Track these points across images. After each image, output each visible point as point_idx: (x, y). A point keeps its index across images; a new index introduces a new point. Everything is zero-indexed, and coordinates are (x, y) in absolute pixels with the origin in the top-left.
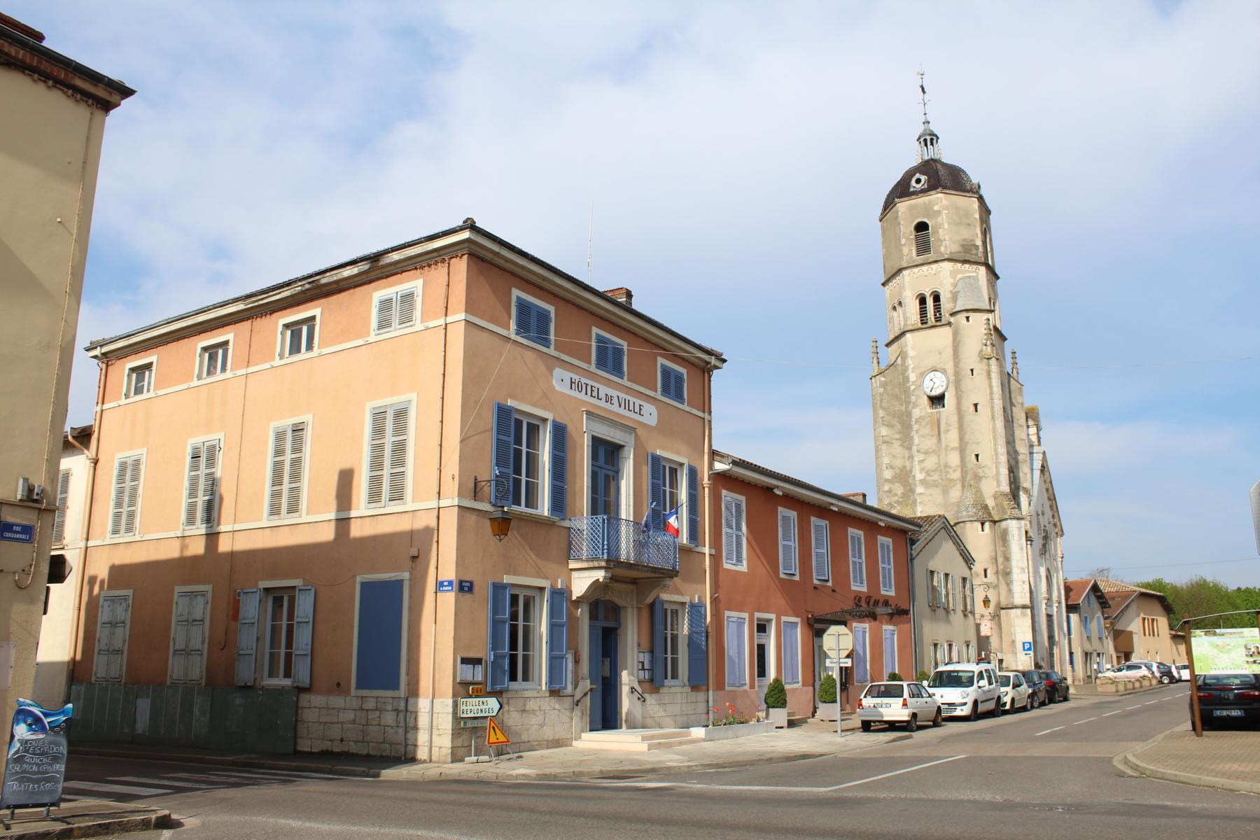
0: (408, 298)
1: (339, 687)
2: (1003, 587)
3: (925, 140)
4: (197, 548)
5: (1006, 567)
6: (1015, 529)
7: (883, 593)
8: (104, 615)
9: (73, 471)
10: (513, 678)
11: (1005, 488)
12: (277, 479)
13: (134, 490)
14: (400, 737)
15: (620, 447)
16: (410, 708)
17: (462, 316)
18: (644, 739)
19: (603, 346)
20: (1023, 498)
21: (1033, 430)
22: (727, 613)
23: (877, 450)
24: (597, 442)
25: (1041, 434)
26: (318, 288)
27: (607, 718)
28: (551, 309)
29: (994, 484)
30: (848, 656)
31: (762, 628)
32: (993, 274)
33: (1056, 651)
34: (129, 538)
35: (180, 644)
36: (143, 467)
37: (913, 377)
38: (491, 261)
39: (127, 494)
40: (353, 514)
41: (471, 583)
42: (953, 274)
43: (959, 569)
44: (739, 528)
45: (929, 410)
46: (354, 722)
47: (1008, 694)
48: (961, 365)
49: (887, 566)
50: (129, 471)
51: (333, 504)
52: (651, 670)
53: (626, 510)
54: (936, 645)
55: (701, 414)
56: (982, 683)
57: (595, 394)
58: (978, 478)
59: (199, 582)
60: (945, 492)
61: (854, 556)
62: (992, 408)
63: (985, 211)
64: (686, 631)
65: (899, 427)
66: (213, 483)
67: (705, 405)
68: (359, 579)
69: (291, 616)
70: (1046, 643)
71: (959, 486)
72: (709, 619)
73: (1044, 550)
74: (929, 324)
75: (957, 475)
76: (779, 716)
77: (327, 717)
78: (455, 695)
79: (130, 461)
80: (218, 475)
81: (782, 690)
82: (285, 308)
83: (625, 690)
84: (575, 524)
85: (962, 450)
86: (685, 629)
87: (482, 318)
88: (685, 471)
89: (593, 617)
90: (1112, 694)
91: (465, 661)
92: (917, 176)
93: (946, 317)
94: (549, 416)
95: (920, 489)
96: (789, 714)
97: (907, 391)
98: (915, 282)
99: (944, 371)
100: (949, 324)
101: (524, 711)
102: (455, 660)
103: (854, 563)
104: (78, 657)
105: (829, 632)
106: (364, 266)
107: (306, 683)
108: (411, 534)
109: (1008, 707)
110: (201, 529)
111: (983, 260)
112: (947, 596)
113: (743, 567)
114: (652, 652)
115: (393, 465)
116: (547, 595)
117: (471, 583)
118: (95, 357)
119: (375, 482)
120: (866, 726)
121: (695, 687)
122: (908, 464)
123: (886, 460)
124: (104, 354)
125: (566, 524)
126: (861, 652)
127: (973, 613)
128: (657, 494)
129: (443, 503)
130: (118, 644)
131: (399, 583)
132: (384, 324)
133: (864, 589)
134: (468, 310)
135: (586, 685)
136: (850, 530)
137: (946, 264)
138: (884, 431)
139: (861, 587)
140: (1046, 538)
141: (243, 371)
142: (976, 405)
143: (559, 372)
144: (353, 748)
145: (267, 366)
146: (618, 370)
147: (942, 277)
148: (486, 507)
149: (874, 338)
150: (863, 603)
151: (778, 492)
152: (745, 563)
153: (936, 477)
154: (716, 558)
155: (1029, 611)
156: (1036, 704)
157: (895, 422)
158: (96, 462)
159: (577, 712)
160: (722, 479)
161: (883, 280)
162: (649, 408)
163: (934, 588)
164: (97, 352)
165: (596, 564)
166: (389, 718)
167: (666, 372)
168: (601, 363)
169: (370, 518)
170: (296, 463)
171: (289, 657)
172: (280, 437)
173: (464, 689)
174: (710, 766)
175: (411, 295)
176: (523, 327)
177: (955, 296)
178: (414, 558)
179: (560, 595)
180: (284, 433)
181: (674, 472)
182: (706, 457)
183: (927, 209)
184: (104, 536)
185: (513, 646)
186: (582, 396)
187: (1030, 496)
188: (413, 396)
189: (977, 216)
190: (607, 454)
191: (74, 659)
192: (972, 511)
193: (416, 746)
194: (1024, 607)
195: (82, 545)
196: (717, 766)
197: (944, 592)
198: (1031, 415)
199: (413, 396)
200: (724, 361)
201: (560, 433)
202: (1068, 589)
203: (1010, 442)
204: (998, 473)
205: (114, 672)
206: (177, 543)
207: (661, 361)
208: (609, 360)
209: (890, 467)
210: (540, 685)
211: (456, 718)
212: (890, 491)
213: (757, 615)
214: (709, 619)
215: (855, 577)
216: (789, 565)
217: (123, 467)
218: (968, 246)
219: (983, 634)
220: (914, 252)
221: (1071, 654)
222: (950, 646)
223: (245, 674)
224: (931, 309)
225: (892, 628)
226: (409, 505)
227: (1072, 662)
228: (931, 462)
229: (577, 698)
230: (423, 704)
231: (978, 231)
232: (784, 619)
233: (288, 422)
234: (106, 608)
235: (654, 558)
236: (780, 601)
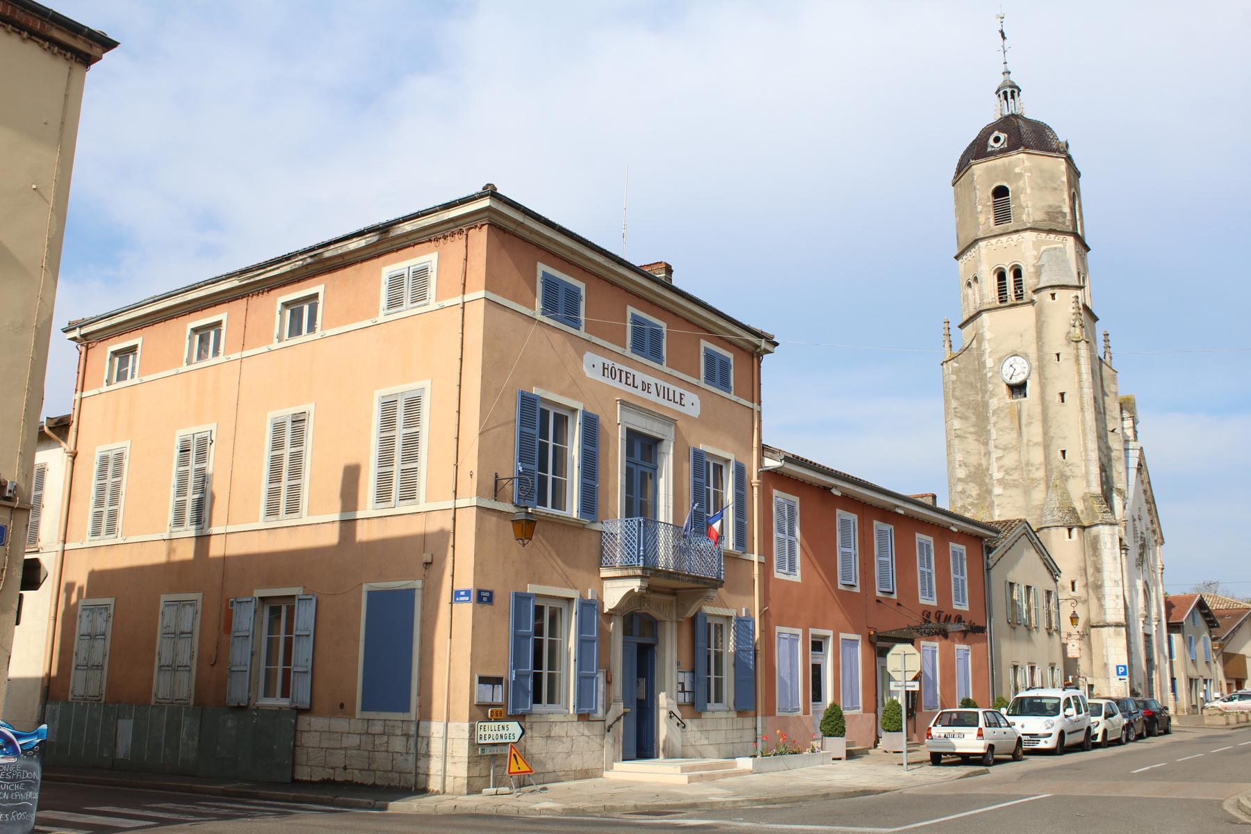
0: (421, 275)
1: (343, 709)
2: (1093, 602)
3: (1005, 93)
4: (186, 552)
5: (1096, 580)
6: (1107, 536)
7: (955, 607)
8: (83, 626)
9: (49, 466)
10: (537, 699)
11: (1096, 489)
12: (275, 476)
13: (117, 486)
14: (410, 766)
15: (658, 441)
16: (422, 733)
17: (482, 293)
18: (684, 770)
19: (639, 327)
20: (1117, 501)
21: (1128, 423)
22: (778, 629)
23: (949, 446)
24: (632, 435)
25: (1138, 426)
26: (320, 262)
27: (642, 745)
28: (581, 286)
30: (915, 679)
31: (818, 646)
32: (1082, 245)
33: (1155, 676)
34: (110, 540)
35: (166, 659)
36: (126, 462)
37: (989, 363)
38: (515, 233)
39: (108, 492)
40: (359, 514)
41: (491, 593)
42: (1036, 245)
43: (1042, 581)
44: (792, 533)
45: (1009, 401)
46: (359, 748)
47: (1099, 725)
48: (1046, 349)
49: (960, 577)
50: (111, 466)
51: (338, 504)
52: (692, 692)
53: (665, 512)
54: (1015, 667)
55: (749, 404)
56: (1070, 711)
57: (630, 381)
58: (1064, 478)
59: (189, 591)
60: (1027, 493)
61: (922, 565)
62: (1081, 397)
63: (1074, 173)
64: (731, 649)
65: (974, 419)
66: (203, 480)
67: (753, 391)
68: (365, 588)
69: (289, 629)
70: (1144, 668)
71: (1042, 486)
72: (757, 636)
73: (1141, 560)
75: (1040, 474)
76: (837, 745)
77: (328, 742)
78: (471, 719)
79: (111, 455)
80: (209, 471)
81: (841, 716)
82: (284, 285)
83: (663, 714)
84: (608, 527)
85: (1046, 446)
86: (730, 646)
87: (504, 296)
88: (732, 468)
89: (627, 631)
90: (1221, 727)
91: (483, 680)
92: (996, 133)
93: (1028, 294)
94: (579, 406)
95: (997, 490)
96: (848, 744)
97: (983, 379)
99: (1025, 356)
100: (1032, 302)
101: (549, 737)
102: (472, 679)
103: (922, 572)
104: (54, 673)
105: (892, 651)
106: (372, 238)
107: (306, 705)
108: (424, 537)
109: (1099, 739)
110: (190, 530)
111: (1071, 229)
112: (1029, 611)
113: (797, 577)
114: (693, 671)
115: (404, 461)
116: (575, 607)
117: (491, 593)
118: (74, 339)
119: (384, 480)
120: (936, 759)
121: (741, 713)
122: (984, 462)
123: (959, 457)
124: (84, 336)
125: (598, 527)
126: (930, 674)
127: (1058, 631)
128: (699, 493)
129: (459, 503)
130: (97, 658)
131: (410, 593)
132: (395, 302)
133: (934, 603)
134: (486, 289)
135: (619, 708)
136: (918, 535)
137: (1028, 234)
138: (957, 424)
139: (929, 601)
140: (1143, 546)
141: (237, 355)
142: (1062, 395)
143: (590, 357)
144: (358, 777)
145: (264, 349)
146: (656, 355)
147: (1023, 249)
148: (508, 507)
149: (945, 318)
150: (933, 619)
151: (836, 492)
152: (798, 572)
153: (1016, 476)
154: (766, 567)
155: (1123, 629)
156: (1132, 737)
157: (970, 413)
158: (74, 456)
159: (609, 739)
160: (774, 478)
161: (956, 253)
162: (691, 398)
163: (1013, 602)
164: (76, 334)
165: (631, 572)
166: (398, 744)
167: (710, 357)
168: (638, 346)
169: (379, 520)
170: (296, 458)
171: (287, 673)
172: (278, 428)
173: (482, 712)
174: (758, 801)
175: (424, 270)
176: (550, 306)
177: (1038, 271)
178: (428, 564)
179: (590, 607)
180: (283, 424)
181: (718, 469)
182: (755, 452)
183: (1007, 172)
184: (83, 538)
185: (538, 663)
186: (615, 383)
187: (1124, 499)
188: (427, 383)
189: (1065, 179)
190: (643, 448)
191: (49, 675)
193: (428, 775)
194: (1118, 625)
195: (59, 547)
196: (767, 801)
197: (1025, 607)
198: (1127, 406)
199: (427, 383)
200: (776, 344)
201: (591, 425)
202: (1169, 605)
203: (1102, 436)
204: (1087, 473)
205: (93, 690)
206: (164, 546)
207: (704, 344)
208: (647, 343)
210: (567, 708)
211: (473, 745)
212: (963, 492)
213: (812, 631)
214: (757, 636)
215: (923, 589)
216: (849, 574)
217: (104, 461)
218: (1054, 214)
219: (1069, 655)
220: (992, 221)
221: (1173, 679)
222: (1032, 668)
223: (238, 692)
224: (1011, 285)
225: (965, 647)
226: (422, 504)
227: (1174, 690)
228: (1010, 459)
229: (609, 722)
230: (437, 728)
231: (1066, 196)
232: (842, 635)
233: (286, 412)
234: (84, 617)
235: (695, 566)
236: (837, 615)
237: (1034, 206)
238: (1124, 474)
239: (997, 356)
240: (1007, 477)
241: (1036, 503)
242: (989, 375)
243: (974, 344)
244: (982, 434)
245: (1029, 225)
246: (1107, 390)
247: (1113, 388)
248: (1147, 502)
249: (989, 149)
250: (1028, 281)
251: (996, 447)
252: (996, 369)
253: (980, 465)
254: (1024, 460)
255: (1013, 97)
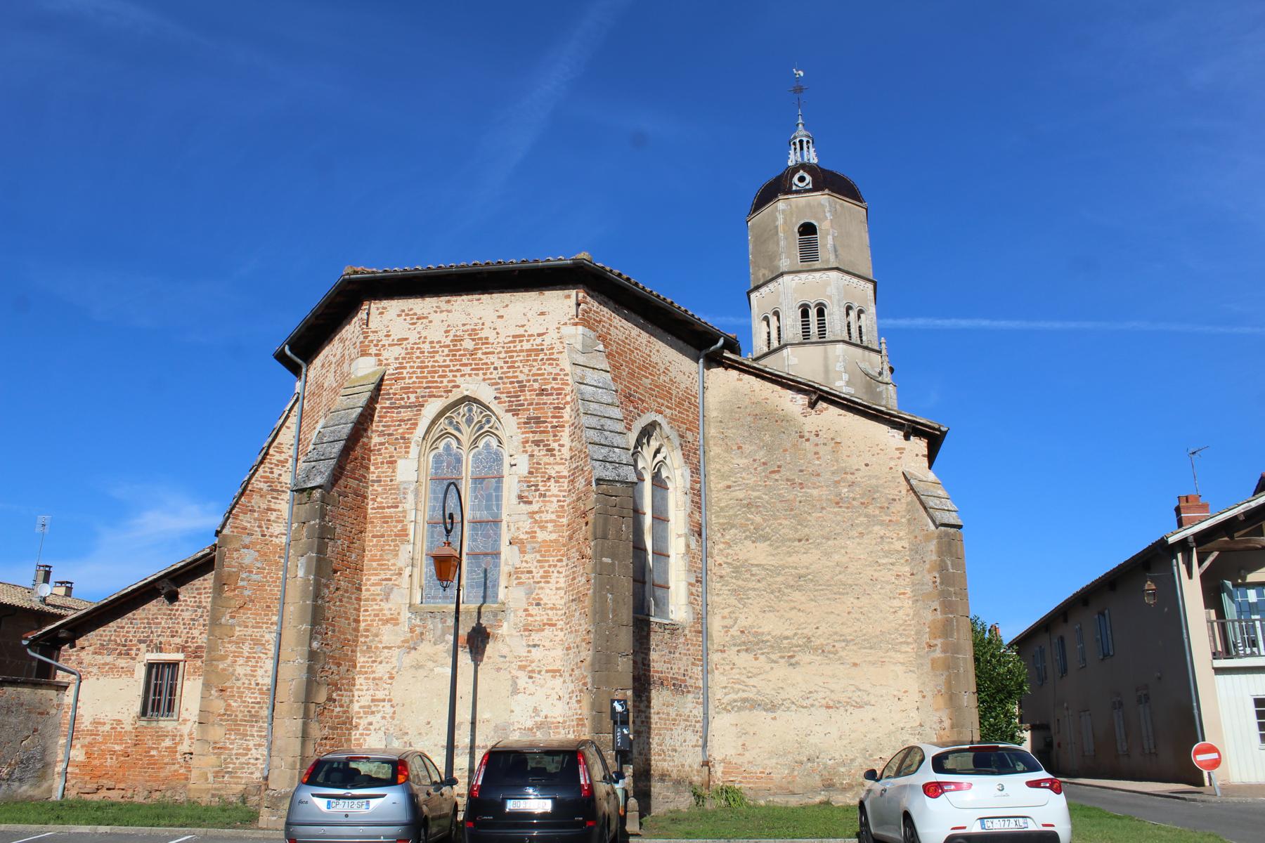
3: (801, 142)
92: (801, 173)
137: (834, 274)
249: (794, 188)
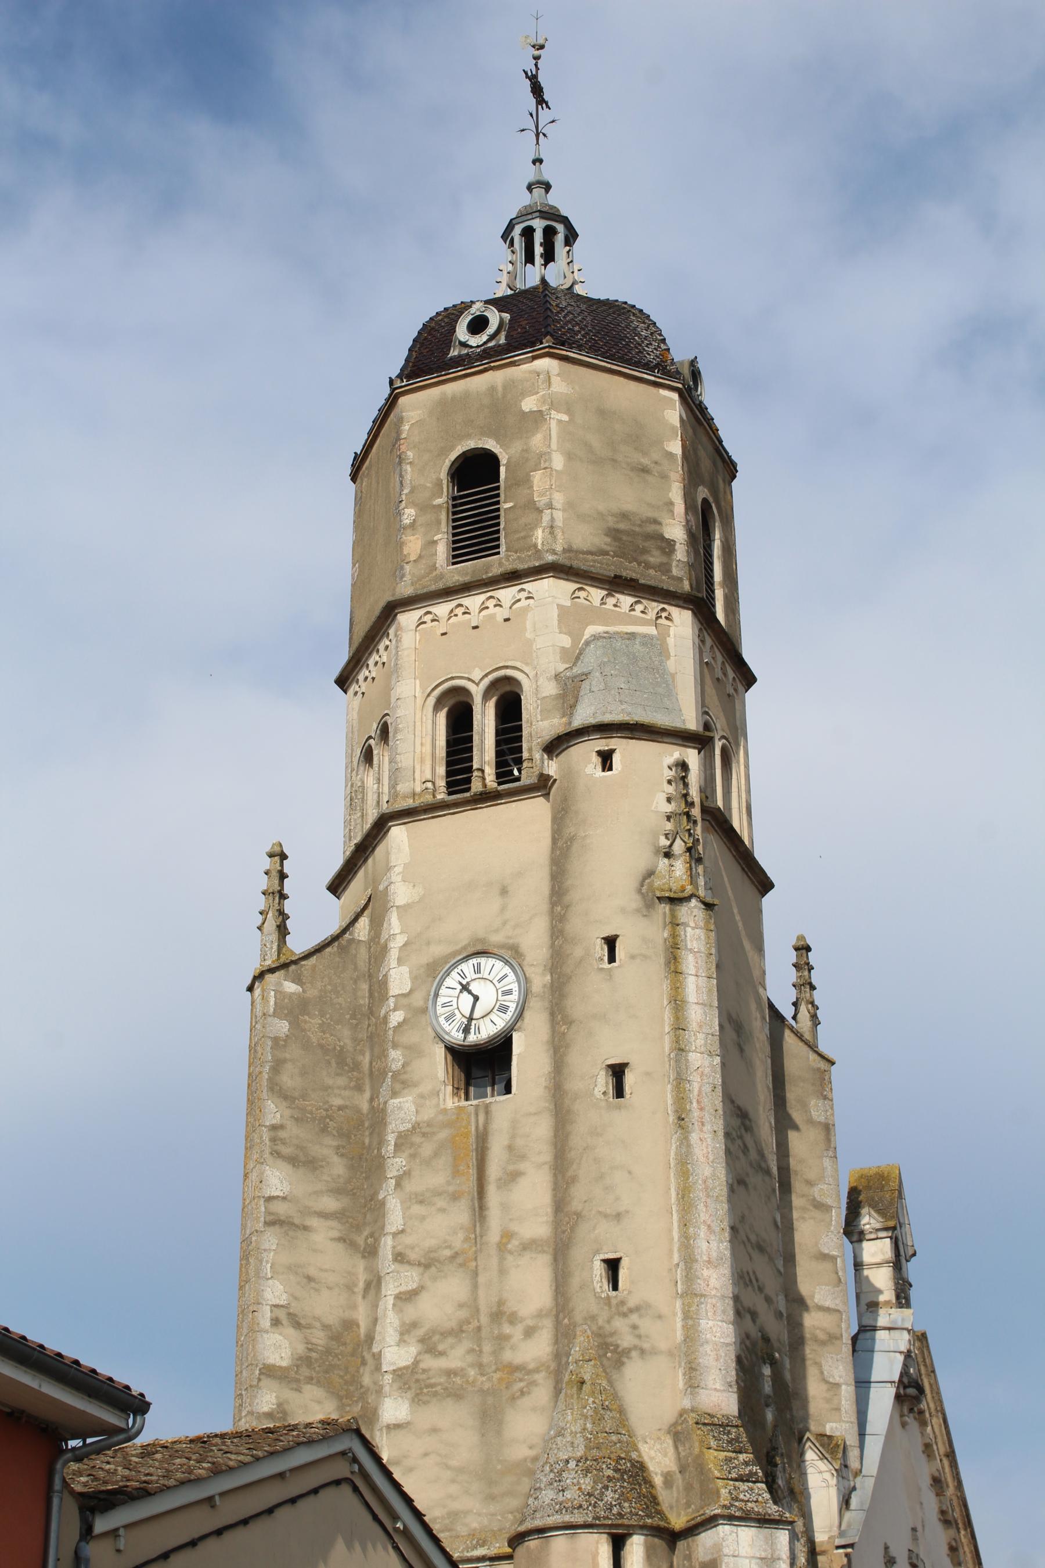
3: (528, 233)
11: (721, 1397)
20: (820, 1479)
21: (876, 1250)
25: (913, 1269)
29: (680, 1376)
37: (399, 979)
42: (570, 619)
45: (450, 1102)
48: (575, 925)
58: (611, 1355)
60: (490, 1420)
62: (680, 1082)
65: (338, 1168)
71: (542, 1393)
74: (476, 786)
75: (537, 1349)
85: (560, 1249)
93: (535, 761)
97: (377, 1037)
98: (438, 649)
99: (512, 955)
100: (543, 785)
123: (275, 1292)
138: (277, 1180)
142: (618, 1072)
147: (533, 632)
153: (456, 1357)
157: (325, 1148)
161: (342, 658)
177: (570, 690)
183: (501, 412)
187: (843, 1471)
189: (676, 447)
192: (578, 1484)
198: (871, 1199)
204: (691, 1336)
209: (289, 1318)
218: (633, 537)
220: (442, 550)
224: (489, 749)
228: (443, 1300)
231: (676, 494)
237: (570, 506)
238: (847, 1392)
239: (424, 958)
240: (430, 1362)
241: (520, 1452)
242: (396, 1018)
243: (362, 929)
244: (360, 1220)
245: (550, 558)
246: (796, 1115)
247: (817, 1110)
248: (947, 1521)
249: (454, 352)
250: (538, 724)
251: (399, 1258)
252: (417, 1000)
253: (350, 1325)
254: (486, 1301)
255: (549, 257)
